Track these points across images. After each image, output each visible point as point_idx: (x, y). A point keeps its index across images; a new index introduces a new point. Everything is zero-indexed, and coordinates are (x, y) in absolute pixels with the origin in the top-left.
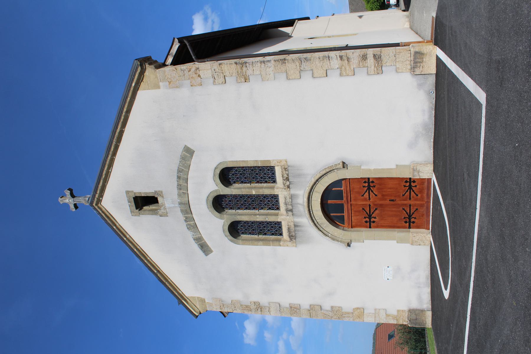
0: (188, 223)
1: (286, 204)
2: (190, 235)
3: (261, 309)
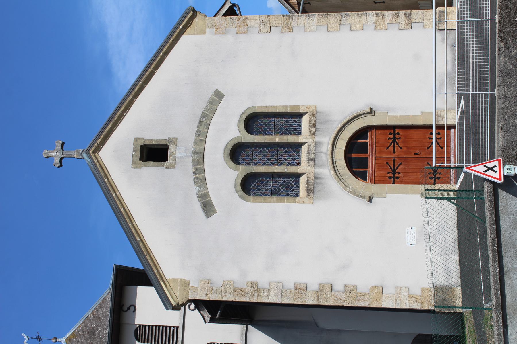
0: (197, 176)
2: (194, 190)
3: (258, 292)
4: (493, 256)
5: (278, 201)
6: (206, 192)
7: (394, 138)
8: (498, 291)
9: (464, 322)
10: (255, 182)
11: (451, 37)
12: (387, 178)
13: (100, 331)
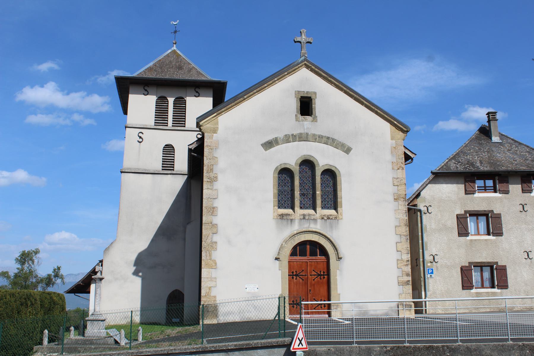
1: (309, 215)
2: (280, 135)
3: (210, 182)
4: (239, 344)
5: (274, 194)
6: (279, 144)
8: (215, 349)
9: (193, 326)
10: (287, 178)
11: (393, 313)
12: (293, 271)
13: (181, 73)
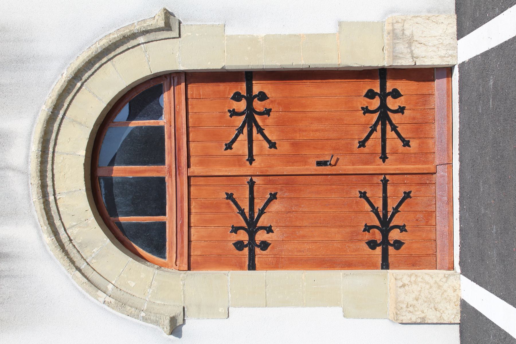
7: (250, 113)
12: (231, 246)
